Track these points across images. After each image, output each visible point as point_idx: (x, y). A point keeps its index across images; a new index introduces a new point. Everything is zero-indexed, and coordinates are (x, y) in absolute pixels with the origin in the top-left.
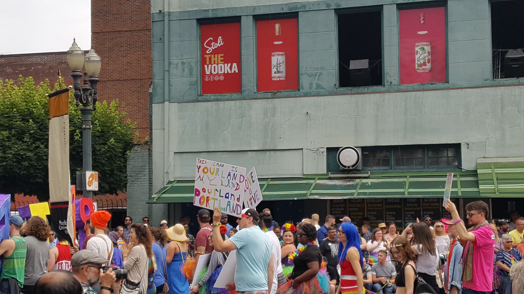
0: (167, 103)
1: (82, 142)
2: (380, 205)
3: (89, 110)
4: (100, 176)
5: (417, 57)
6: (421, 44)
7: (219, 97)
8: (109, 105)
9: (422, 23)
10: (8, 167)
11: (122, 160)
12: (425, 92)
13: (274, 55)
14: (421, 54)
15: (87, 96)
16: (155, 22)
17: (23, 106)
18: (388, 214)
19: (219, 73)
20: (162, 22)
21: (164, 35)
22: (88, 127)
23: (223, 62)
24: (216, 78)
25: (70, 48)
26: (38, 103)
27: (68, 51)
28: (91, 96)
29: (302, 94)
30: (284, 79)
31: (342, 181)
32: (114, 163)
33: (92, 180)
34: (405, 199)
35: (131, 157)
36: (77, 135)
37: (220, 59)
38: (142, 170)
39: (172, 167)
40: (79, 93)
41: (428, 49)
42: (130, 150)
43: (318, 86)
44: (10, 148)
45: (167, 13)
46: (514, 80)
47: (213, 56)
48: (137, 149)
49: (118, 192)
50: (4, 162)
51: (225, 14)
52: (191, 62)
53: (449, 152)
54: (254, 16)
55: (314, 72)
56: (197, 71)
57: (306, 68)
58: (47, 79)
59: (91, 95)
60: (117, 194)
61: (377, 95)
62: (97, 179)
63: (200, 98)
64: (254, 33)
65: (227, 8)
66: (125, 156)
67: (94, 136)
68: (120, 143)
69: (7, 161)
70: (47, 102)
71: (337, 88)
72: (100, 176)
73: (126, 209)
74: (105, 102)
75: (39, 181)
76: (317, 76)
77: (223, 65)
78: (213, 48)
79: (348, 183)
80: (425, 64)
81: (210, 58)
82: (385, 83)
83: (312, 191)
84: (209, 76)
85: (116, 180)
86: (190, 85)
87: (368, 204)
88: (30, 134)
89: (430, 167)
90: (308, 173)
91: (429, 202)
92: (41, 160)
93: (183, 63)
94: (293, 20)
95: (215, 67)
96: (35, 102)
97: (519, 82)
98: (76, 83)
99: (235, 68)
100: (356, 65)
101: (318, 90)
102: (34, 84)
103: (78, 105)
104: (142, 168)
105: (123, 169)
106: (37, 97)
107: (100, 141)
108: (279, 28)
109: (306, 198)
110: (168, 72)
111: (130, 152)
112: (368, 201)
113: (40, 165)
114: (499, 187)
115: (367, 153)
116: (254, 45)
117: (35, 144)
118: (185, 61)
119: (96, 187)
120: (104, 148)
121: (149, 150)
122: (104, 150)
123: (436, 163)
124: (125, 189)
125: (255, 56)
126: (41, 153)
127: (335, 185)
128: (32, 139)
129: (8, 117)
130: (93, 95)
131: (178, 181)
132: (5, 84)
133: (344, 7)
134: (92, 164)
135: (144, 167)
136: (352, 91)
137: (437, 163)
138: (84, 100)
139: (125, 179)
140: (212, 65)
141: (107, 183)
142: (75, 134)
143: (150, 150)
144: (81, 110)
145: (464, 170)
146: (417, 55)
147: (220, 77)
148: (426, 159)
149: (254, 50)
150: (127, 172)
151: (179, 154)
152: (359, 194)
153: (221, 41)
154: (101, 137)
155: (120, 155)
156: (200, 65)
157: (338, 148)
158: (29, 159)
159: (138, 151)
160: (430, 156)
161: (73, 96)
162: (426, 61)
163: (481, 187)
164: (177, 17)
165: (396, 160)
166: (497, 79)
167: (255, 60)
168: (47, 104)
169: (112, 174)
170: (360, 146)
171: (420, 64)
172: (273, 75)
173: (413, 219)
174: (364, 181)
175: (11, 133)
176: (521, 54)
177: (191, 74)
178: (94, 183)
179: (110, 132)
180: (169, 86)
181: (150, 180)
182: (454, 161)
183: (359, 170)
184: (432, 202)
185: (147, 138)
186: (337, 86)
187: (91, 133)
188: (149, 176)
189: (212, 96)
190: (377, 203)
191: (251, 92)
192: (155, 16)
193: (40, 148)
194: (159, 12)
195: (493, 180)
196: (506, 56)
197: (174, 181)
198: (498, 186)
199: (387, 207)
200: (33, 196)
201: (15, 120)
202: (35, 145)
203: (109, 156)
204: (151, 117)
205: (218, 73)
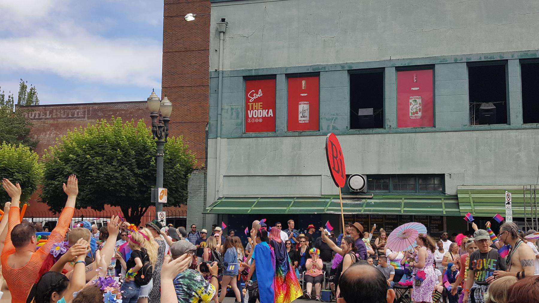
1: (156, 167)
3: (162, 142)
7: (258, 135)
8: (176, 138)
10: (100, 184)
11: (184, 180)
12: (417, 134)
15: (161, 131)
17: (113, 138)
18: (387, 227)
20: (218, 78)
22: (161, 155)
25: (150, 96)
26: (124, 137)
27: (148, 99)
29: (321, 134)
30: (308, 122)
31: (352, 200)
33: (163, 194)
34: (401, 216)
36: (153, 161)
39: (222, 187)
43: (334, 128)
44: (102, 170)
46: (486, 126)
49: (181, 205)
50: (97, 180)
55: (331, 117)
59: (164, 131)
60: (180, 207)
61: (380, 135)
62: (167, 194)
63: (244, 135)
67: (165, 162)
68: (183, 167)
69: (99, 179)
73: (186, 218)
74: (173, 138)
79: (356, 202)
84: (251, 119)
85: (180, 196)
87: (372, 219)
88: (118, 160)
89: (421, 191)
91: (419, 219)
94: (316, 77)
97: (490, 128)
103: (154, 138)
105: (185, 187)
109: (324, 213)
113: (124, 183)
115: (371, 180)
116: (286, 96)
117: (121, 167)
120: (172, 171)
121: (205, 174)
124: (186, 203)
126: (125, 174)
127: (346, 203)
128: (119, 163)
129: (102, 147)
130: (165, 131)
132: (100, 123)
135: (201, 187)
138: (159, 135)
141: (173, 197)
142: (151, 161)
143: (205, 174)
144: (156, 142)
145: (447, 195)
149: (286, 100)
151: (228, 177)
152: (365, 211)
155: (183, 176)
157: (349, 175)
158: (116, 178)
159: (196, 174)
162: (418, 110)
165: (394, 186)
169: (177, 191)
174: (369, 201)
175: (103, 159)
181: (205, 196)
183: (364, 193)
184: (422, 219)
185: (203, 165)
189: (253, 134)
190: (378, 218)
192: (212, 74)
196: (482, 108)
200: (117, 206)
201: (106, 149)
204: (207, 148)
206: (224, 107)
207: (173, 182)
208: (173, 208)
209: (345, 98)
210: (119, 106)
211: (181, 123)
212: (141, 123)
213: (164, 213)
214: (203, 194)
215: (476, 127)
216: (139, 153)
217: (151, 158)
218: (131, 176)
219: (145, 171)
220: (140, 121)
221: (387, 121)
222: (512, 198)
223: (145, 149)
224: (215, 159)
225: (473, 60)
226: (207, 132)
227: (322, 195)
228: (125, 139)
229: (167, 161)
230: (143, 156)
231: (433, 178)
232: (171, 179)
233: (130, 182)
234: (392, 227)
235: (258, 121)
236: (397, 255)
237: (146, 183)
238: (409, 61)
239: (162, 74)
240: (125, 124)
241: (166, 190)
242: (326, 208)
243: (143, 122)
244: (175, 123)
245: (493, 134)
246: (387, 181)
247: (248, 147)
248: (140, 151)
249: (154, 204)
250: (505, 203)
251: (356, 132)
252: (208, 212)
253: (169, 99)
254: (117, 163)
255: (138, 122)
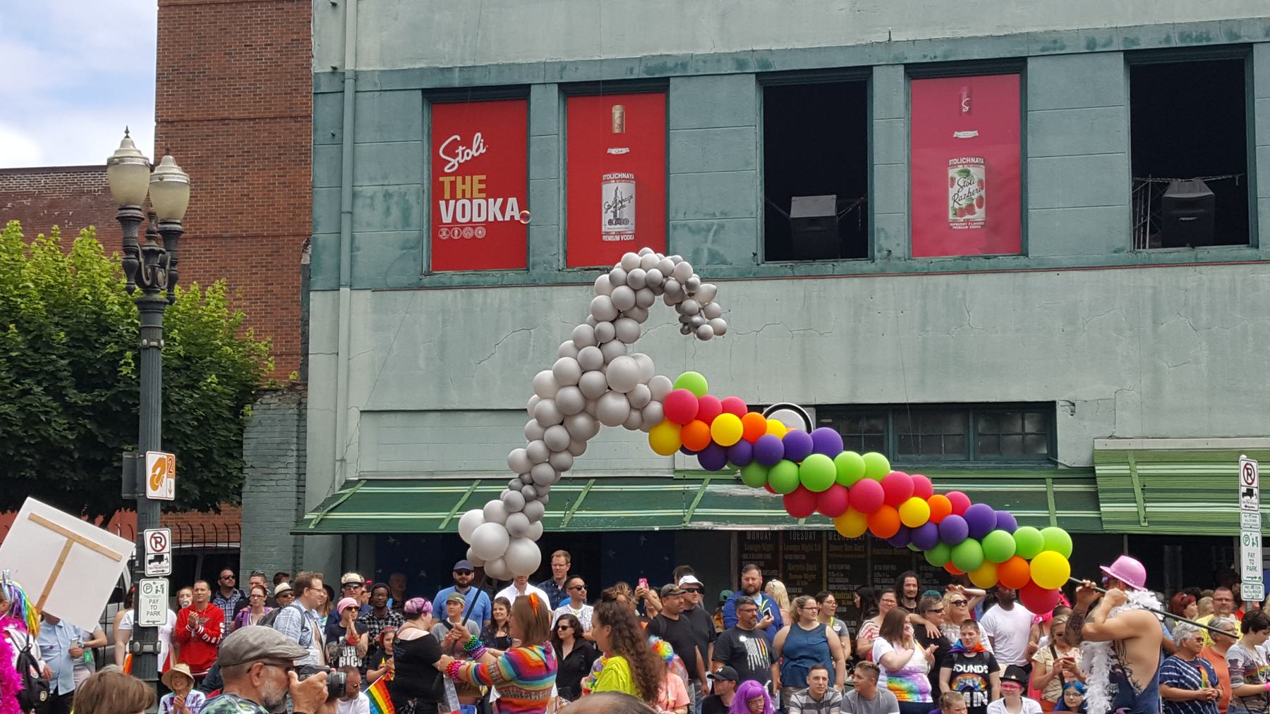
0: (345, 291)
1: (139, 384)
2: (858, 548)
3: (157, 302)
4: (179, 465)
5: (952, 191)
6: (962, 160)
7: (474, 278)
8: (203, 289)
9: (964, 110)
11: (232, 426)
12: (970, 276)
13: (608, 181)
14: (962, 185)
15: (153, 268)
16: (320, 95)
19: (474, 220)
21: (342, 128)
22: (155, 344)
23: (484, 195)
24: (468, 234)
25: (116, 152)
26: (31, 285)
28: (165, 268)
30: (631, 238)
32: (213, 433)
33: (162, 472)
35: (255, 421)
36: (129, 364)
37: (477, 186)
38: (282, 453)
39: (354, 448)
40: (136, 261)
41: (978, 173)
42: (253, 403)
43: (714, 256)
45: (352, 73)
47: (459, 179)
48: (272, 401)
49: (224, 506)
51: (493, 80)
52: (406, 193)
53: (1026, 422)
54: (560, 85)
55: (703, 223)
56: (422, 215)
57: (685, 214)
58: (56, 227)
59: (163, 265)
60: (218, 511)
61: (856, 280)
62: (173, 470)
63: (426, 280)
64: (561, 128)
65: (497, 65)
66: (241, 417)
67: (166, 368)
68: (228, 385)
70: (52, 283)
71: (759, 262)
72: (179, 465)
73: (239, 549)
74: (195, 287)
75: (28, 475)
76: (712, 233)
77: (483, 202)
78: (461, 161)
80: (970, 209)
81: (453, 184)
82: (876, 253)
83: (697, 510)
84: (450, 228)
85: (218, 477)
86: (402, 249)
88: (10, 359)
89: (982, 457)
90: (687, 468)
92: (36, 423)
93: (387, 196)
95: (464, 205)
96: (26, 281)
97: (1196, 258)
98: (128, 235)
99: (512, 210)
100: (805, 207)
101: (713, 267)
102: (23, 239)
103: (130, 291)
104: (283, 447)
105: (234, 448)
106: (28, 270)
107: (182, 380)
108: (622, 117)
109: (681, 526)
110: (349, 215)
111: (252, 409)
112: (830, 539)
113: (32, 437)
114: (1147, 509)
116: (561, 153)
117: (22, 384)
118: (391, 189)
119: (170, 492)
120: (192, 397)
121: (300, 404)
122: (190, 401)
123: (996, 447)
124: (237, 498)
125: (561, 181)
126: (37, 407)
127: (752, 497)
128: (14, 370)
130: (168, 267)
131: (368, 480)
133: (778, 69)
134: (162, 438)
136: (795, 271)
137: (998, 448)
138: (148, 279)
139: (240, 475)
140: (457, 200)
141: (195, 482)
142: (122, 362)
143: (302, 405)
144: (138, 303)
146: (952, 187)
147: (476, 230)
148: (972, 437)
149: (561, 167)
150: (244, 458)
153: (482, 145)
154: (183, 371)
155: (227, 414)
156: (428, 201)
159: (272, 406)
160: (980, 431)
161: (118, 266)
162: (974, 202)
163: (1105, 507)
164: (376, 84)
166: (1141, 250)
167: (562, 192)
168: (52, 287)
169: (208, 461)
170: (814, 403)
171: (961, 209)
172: (606, 227)
173: (938, 582)
176: (1200, 191)
177: (406, 221)
178: (164, 480)
179: (206, 357)
180: (352, 251)
181: (301, 476)
182: (1038, 444)
186: (760, 256)
187: (161, 359)
188: (298, 468)
189: (456, 277)
191: (552, 268)
193: (31, 394)
194: (330, 70)
195: (1132, 491)
196: (1167, 195)
197: (360, 480)
198: (1145, 507)
199: (877, 552)
202: (21, 388)
203: (201, 415)
204: (306, 322)
205: (471, 221)
206: (360, 189)
207: (195, 433)
208: (194, 517)
209: (747, 164)
210: (13, 183)
211: (221, 237)
212: (86, 241)
213: (167, 533)
214: (295, 470)
215: (1153, 256)
216: (81, 337)
217: (121, 354)
218: (55, 413)
219: (101, 396)
220: (83, 235)
221: (879, 239)
222: (1261, 476)
223: (103, 326)
224: (335, 355)
225: (1143, 46)
226: (306, 272)
227: (676, 471)
228: (35, 293)
229: (176, 362)
230: (94, 349)
231: (1019, 415)
232: (189, 425)
233: (52, 431)
234: (893, 568)
235: (471, 235)
236: (912, 655)
237: (105, 437)
238: (946, 47)
239: (158, 78)
240: (34, 244)
241: (170, 458)
242: (688, 513)
243: (91, 237)
244: (200, 238)
245: (1203, 276)
246: (879, 424)
247: (440, 318)
248: (83, 332)
249: (132, 505)
250: (1237, 491)
251: (782, 272)
252: (311, 527)
253: (179, 162)
254: (7, 371)
255: (78, 239)
